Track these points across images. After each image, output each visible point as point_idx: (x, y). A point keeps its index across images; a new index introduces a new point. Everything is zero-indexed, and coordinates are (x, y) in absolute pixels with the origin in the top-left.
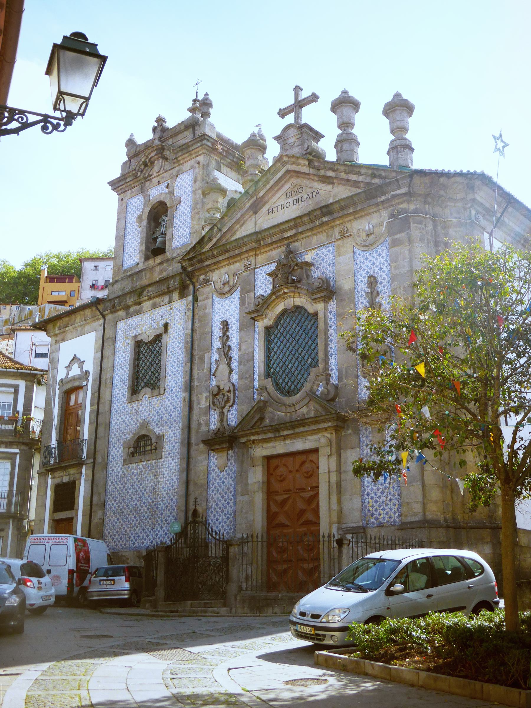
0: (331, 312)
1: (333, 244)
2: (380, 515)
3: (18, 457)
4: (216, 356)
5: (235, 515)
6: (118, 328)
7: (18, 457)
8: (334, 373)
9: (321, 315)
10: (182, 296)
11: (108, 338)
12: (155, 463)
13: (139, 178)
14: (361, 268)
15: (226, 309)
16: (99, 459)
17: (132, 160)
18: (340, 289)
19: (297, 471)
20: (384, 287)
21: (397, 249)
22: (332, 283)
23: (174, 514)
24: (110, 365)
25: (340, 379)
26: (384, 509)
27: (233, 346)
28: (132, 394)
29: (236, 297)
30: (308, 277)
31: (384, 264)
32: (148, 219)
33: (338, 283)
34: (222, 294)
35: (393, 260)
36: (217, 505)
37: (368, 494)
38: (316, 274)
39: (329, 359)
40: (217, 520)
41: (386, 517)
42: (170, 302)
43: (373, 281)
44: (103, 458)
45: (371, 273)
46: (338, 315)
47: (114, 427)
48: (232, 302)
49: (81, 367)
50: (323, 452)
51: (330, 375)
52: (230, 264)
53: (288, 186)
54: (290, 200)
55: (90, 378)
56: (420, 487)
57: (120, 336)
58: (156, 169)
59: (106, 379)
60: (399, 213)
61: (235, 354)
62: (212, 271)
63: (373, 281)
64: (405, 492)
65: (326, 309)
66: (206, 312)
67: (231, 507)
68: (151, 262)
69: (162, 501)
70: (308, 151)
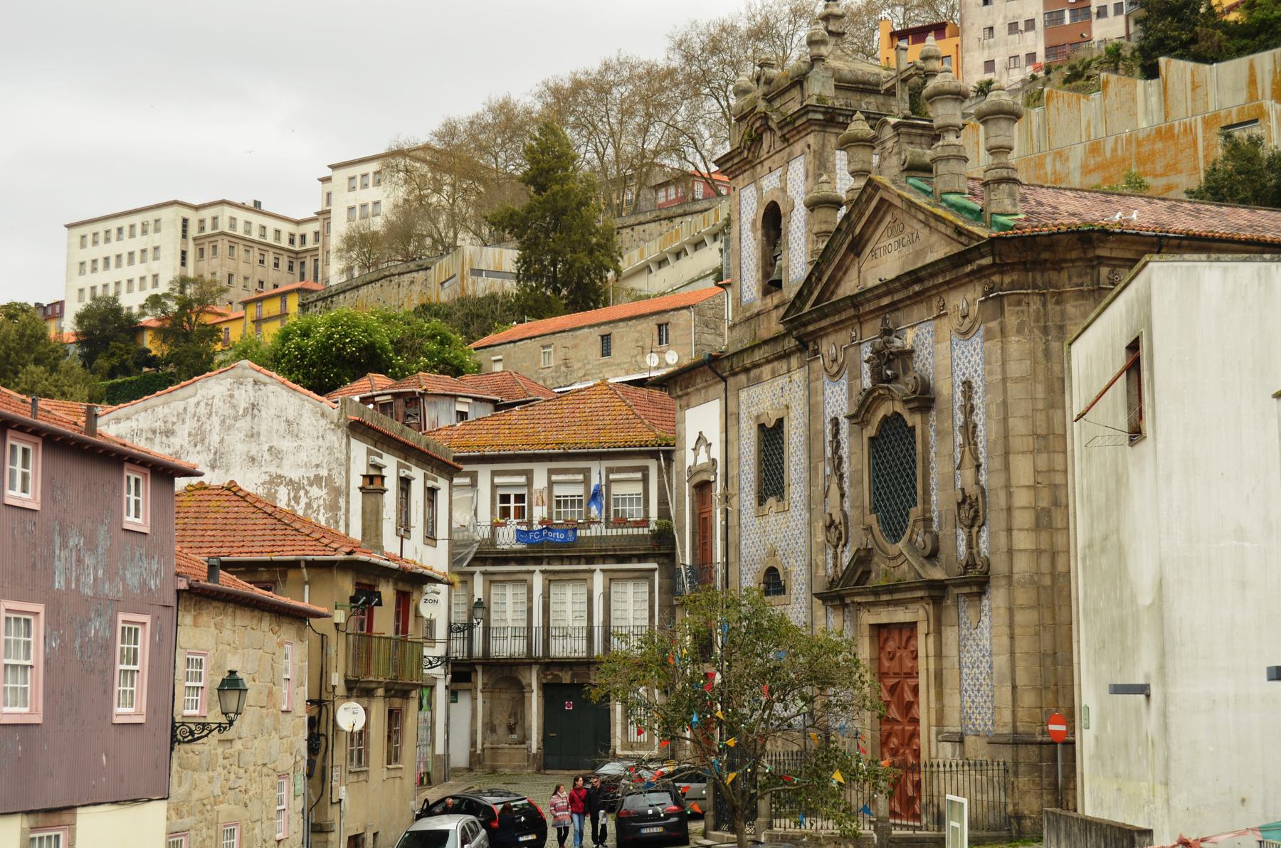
8: (935, 515)
9: (918, 432)
15: (838, 400)
24: (736, 456)
25: (940, 526)
27: (845, 456)
28: (760, 505)
29: (844, 382)
32: (763, 227)
46: (938, 433)
47: (744, 551)
49: (708, 452)
51: (931, 520)
52: (836, 331)
54: (892, 241)
55: (718, 471)
61: (846, 467)
64: (997, 694)
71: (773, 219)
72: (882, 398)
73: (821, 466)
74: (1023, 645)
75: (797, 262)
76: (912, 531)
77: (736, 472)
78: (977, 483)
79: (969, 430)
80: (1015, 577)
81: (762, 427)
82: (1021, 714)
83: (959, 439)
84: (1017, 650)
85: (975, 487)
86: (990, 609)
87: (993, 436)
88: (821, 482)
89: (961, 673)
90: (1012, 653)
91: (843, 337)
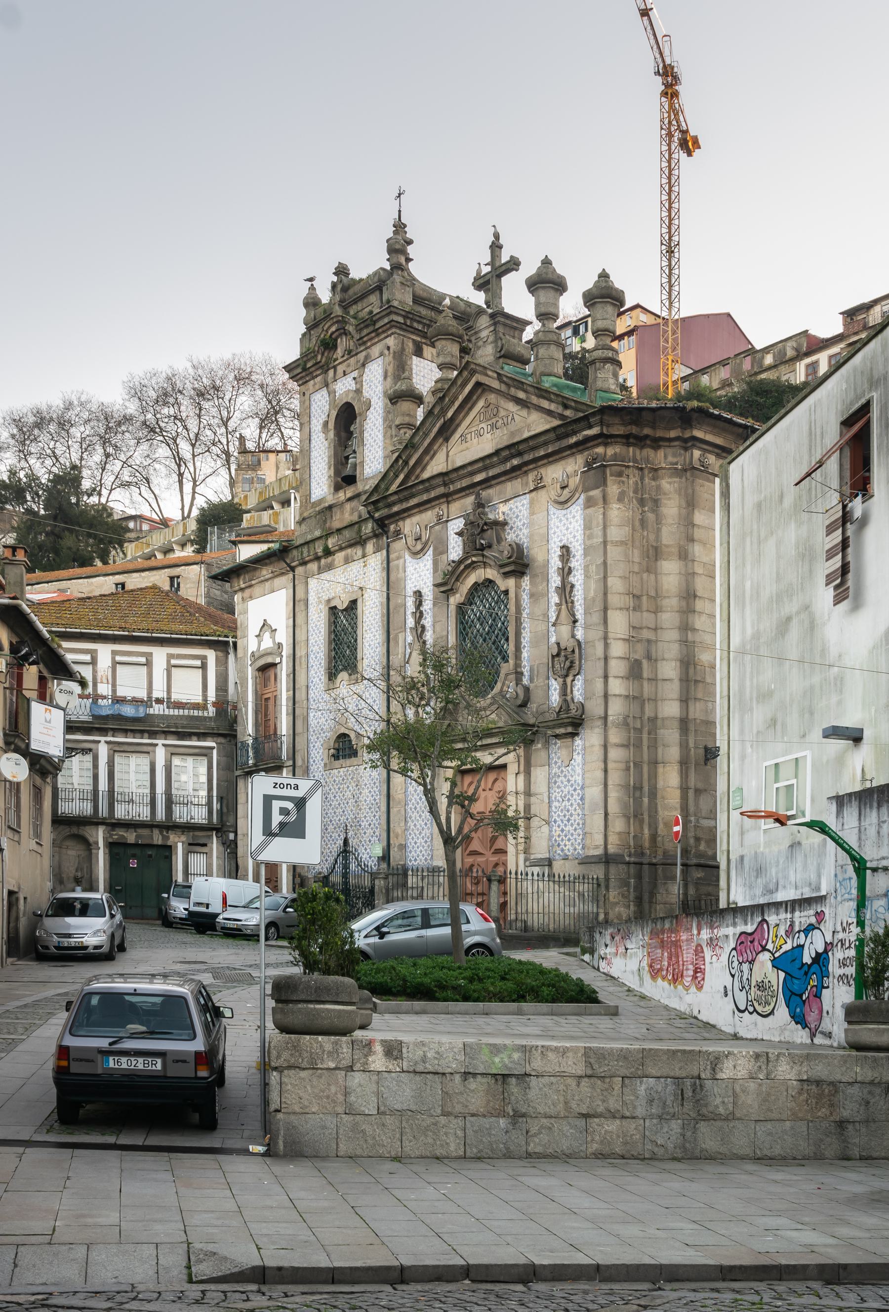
0: (524, 591)
1: (527, 495)
2: (565, 845)
3: (215, 751)
4: (410, 639)
5: (432, 839)
6: (310, 587)
7: (215, 751)
8: (526, 671)
9: (512, 595)
10: (377, 550)
11: (299, 601)
12: (356, 769)
13: (321, 364)
14: (554, 533)
15: (420, 574)
16: (299, 762)
17: (312, 332)
18: (534, 560)
19: (490, 790)
20: (577, 561)
21: (590, 511)
22: (525, 551)
23: (377, 833)
24: (304, 638)
25: (531, 680)
26: (569, 840)
28: (330, 680)
30: (499, 540)
31: (578, 531)
33: (532, 552)
34: (417, 554)
35: (587, 526)
36: (415, 825)
37: (555, 821)
38: (510, 537)
39: (521, 653)
40: (416, 843)
41: (571, 848)
42: (364, 556)
43: (566, 551)
44: (303, 760)
45: (565, 542)
46: (532, 595)
47: (313, 722)
48: (425, 565)
49: (273, 638)
50: (512, 768)
51: (522, 674)
52: (421, 512)
53: (481, 403)
55: (284, 653)
56: (603, 816)
57: (312, 598)
58: (339, 351)
59: (301, 657)
60: (595, 460)
62: (403, 519)
63: (566, 551)
64: (588, 821)
65: (518, 586)
66: (400, 576)
67: (428, 828)
68: (341, 496)
69: (365, 817)
70: (503, 352)
71: (347, 419)
72: (472, 566)
73: (401, 637)
74: (615, 778)
75: (374, 456)
76: (503, 684)
77: (303, 653)
78: (573, 636)
79: (566, 590)
80: (610, 718)
81: (333, 610)
82: (613, 839)
83: (555, 599)
84: (610, 782)
85: (572, 640)
86: (584, 749)
87: (592, 594)
88: (401, 650)
89: (550, 807)
90: (606, 785)
91: (429, 516)
